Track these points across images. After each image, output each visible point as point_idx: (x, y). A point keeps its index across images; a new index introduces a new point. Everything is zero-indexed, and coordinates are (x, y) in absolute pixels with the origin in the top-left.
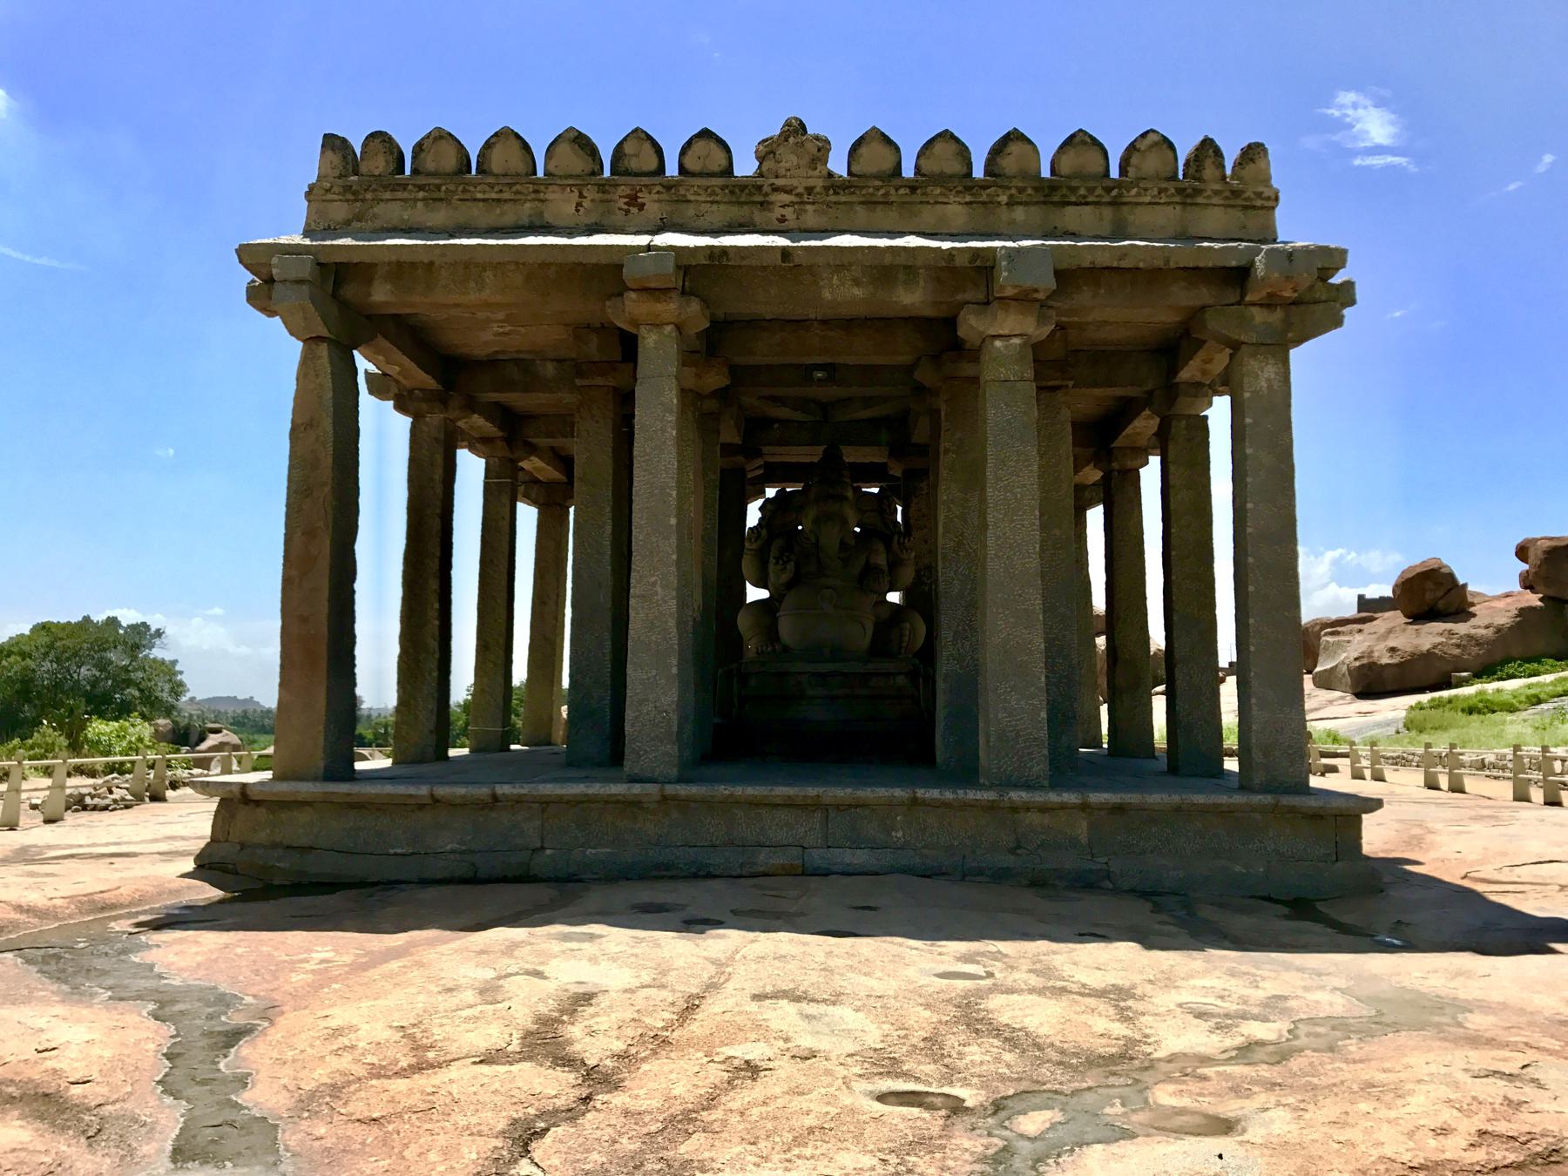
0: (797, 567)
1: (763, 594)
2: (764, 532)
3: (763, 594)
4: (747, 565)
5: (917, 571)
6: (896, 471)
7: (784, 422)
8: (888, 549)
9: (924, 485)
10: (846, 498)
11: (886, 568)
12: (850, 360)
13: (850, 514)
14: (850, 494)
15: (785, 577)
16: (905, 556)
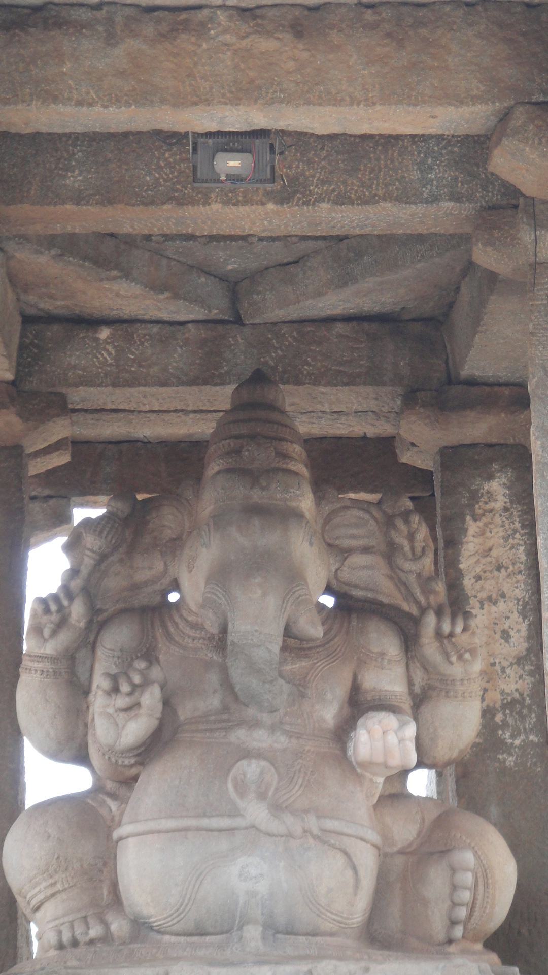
0: (167, 703)
1: (76, 779)
2: (77, 611)
3: (76, 779)
4: (33, 699)
5: (488, 713)
6: (422, 441)
7: (124, 324)
8: (409, 641)
9: (498, 488)
10: (298, 515)
11: (407, 705)
12: (319, 120)
13: (305, 551)
14: (306, 502)
15: (135, 730)
16: (456, 670)
